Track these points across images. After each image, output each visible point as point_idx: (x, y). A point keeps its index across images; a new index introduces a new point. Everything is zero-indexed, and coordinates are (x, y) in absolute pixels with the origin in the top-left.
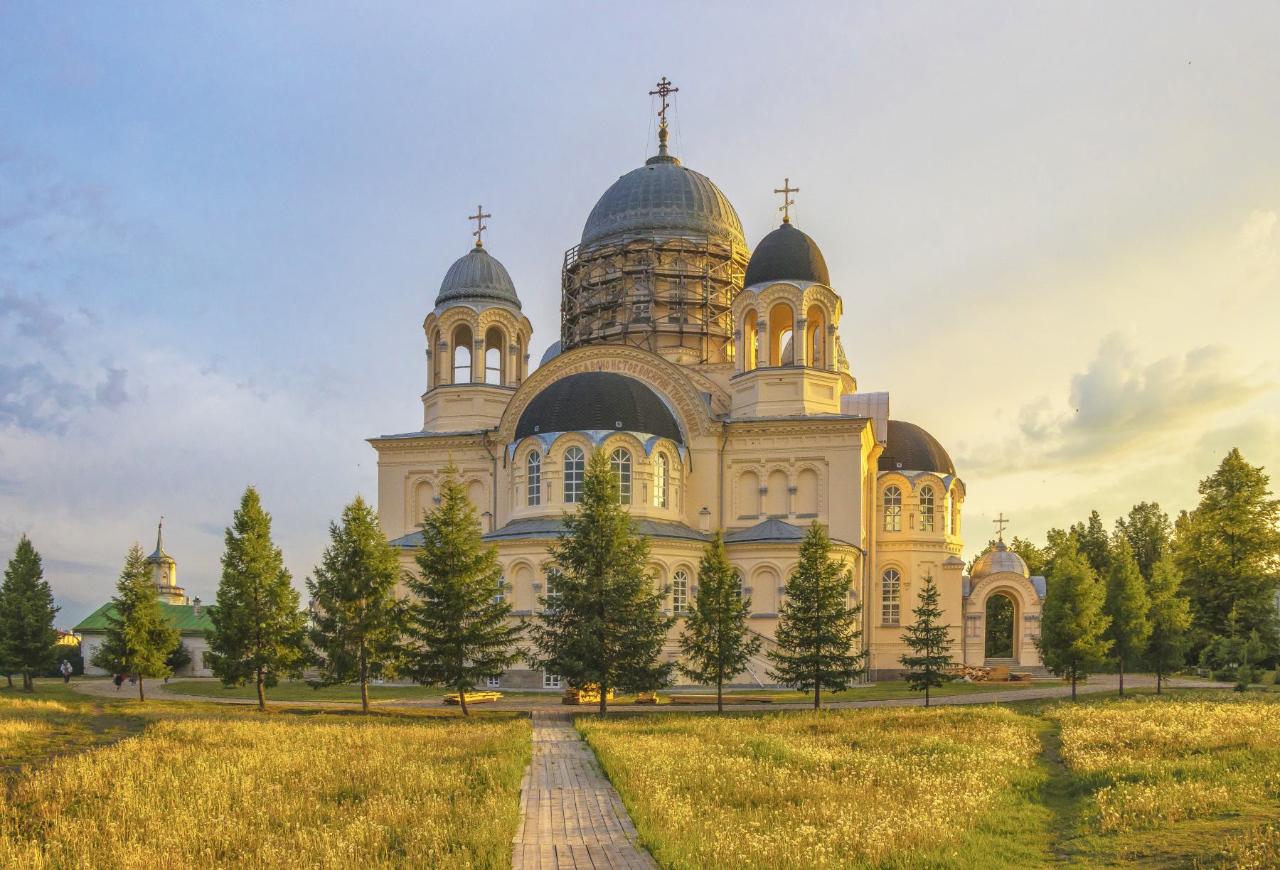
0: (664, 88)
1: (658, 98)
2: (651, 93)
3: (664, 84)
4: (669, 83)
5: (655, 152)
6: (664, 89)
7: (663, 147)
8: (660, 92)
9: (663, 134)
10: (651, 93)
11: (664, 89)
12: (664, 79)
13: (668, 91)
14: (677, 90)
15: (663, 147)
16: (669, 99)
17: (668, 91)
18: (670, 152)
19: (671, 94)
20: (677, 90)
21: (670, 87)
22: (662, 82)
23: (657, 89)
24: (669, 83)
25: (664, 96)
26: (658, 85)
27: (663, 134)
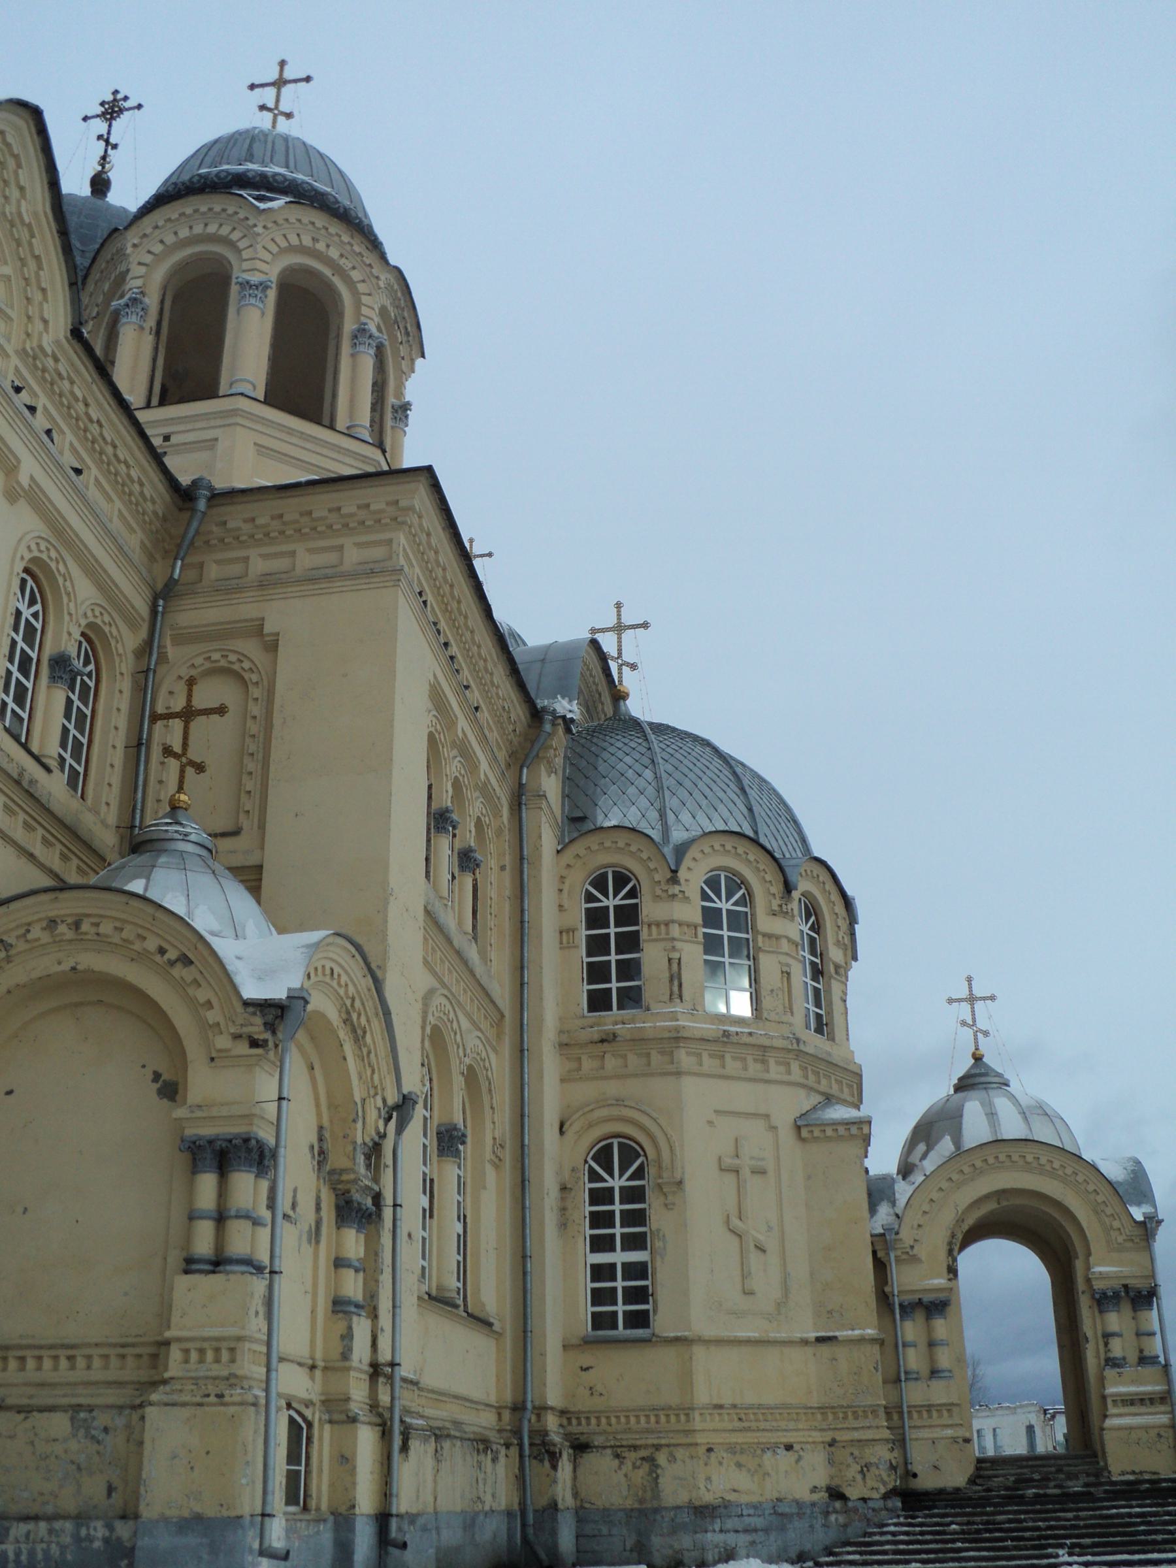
0: (114, 106)
1: (100, 126)
3: (115, 100)
4: (126, 98)
6: (112, 110)
8: (104, 114)
10: (85, 119)
11: (112, 110)
12: (116, 92)
14: (139, 107)
17: (121, 111)
19: (126, 115)
20: (139, 107)
21: (127, 104)
22: (110, 98)
23: (99, 110)
24: (126, 98)
25: (112, 118)
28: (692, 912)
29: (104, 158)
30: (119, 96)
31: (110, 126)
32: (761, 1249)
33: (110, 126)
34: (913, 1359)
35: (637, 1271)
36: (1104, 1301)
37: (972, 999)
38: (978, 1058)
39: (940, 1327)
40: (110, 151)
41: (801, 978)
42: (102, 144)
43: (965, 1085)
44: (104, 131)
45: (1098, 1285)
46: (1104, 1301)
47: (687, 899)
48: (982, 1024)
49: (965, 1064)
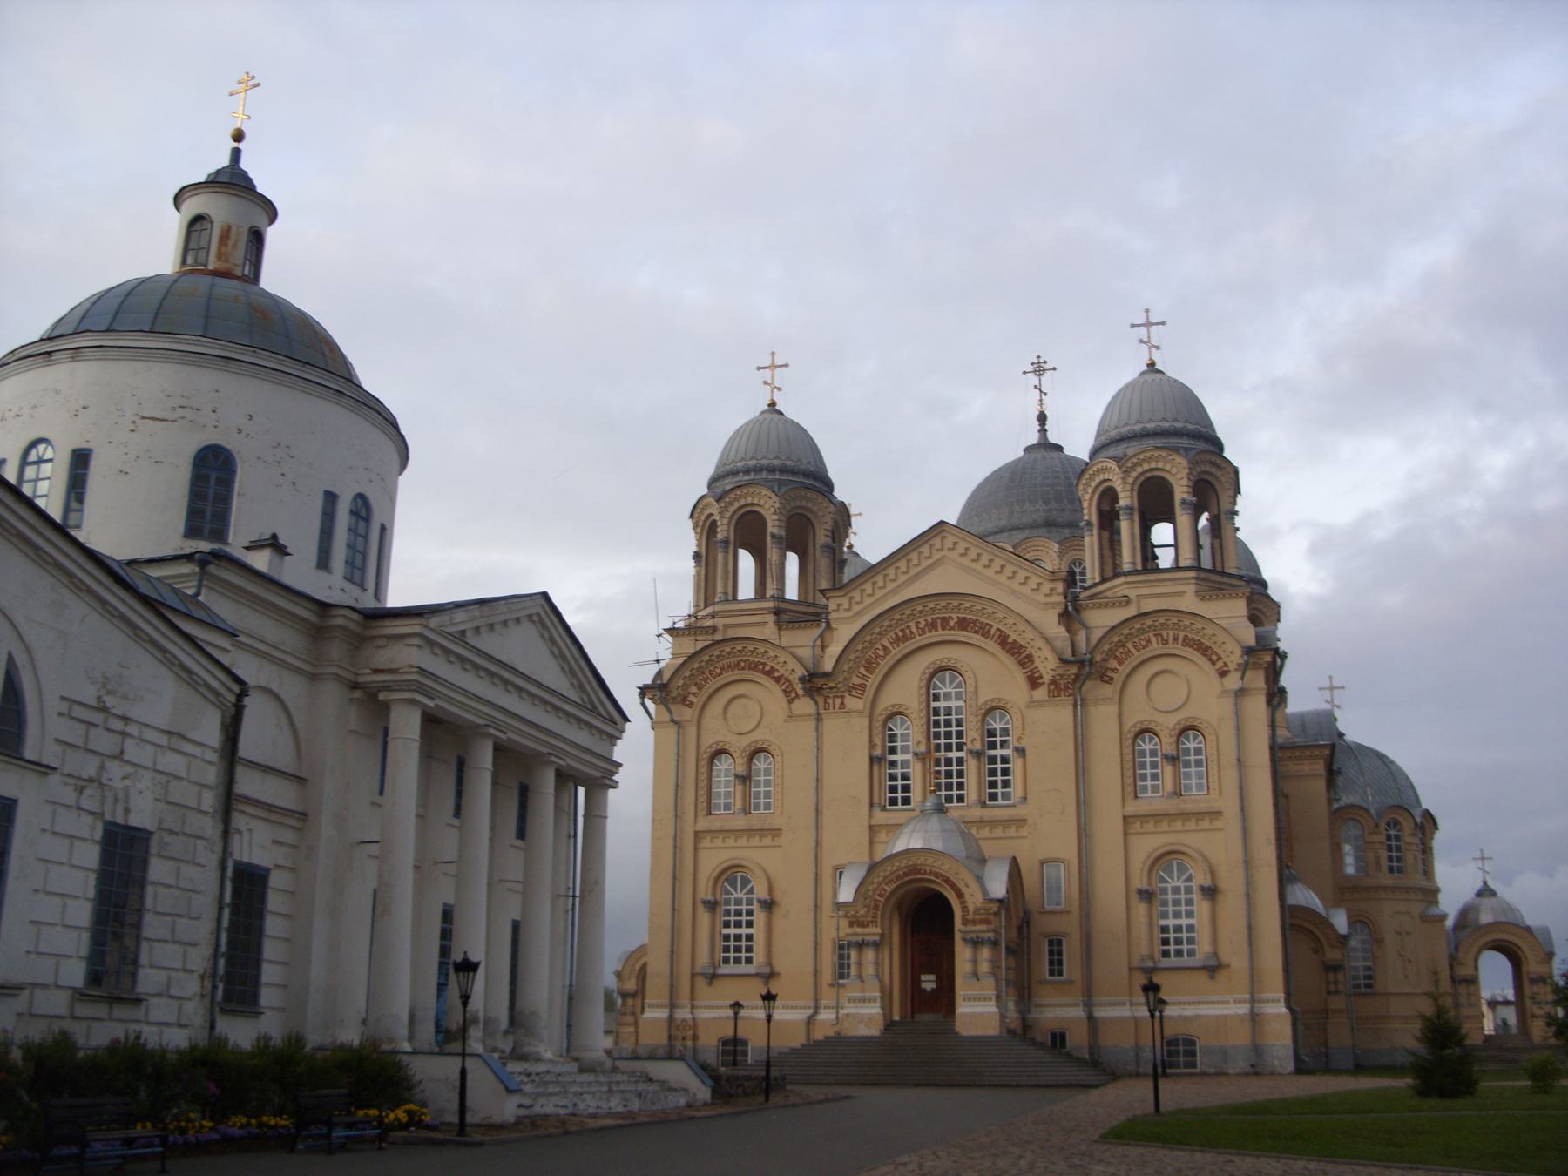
1: (1034, 379)
2: (1025, 373)
3: (1039, 363)
4: (1045, 362)
5: (1034, 439)
6: (1039, 369)
7: (1043, 431)
8: (1035, 371)
9: (1042, 418)
10: (1025, 373)
13: (1044, 370)
14: (1054, 369)
15: (1043, 431)
16: (1046, 377)
17: (1044, 370)
18: (1053, 438)
20: (1054, 369)
21: (1047, 366)
22: (1036, 361)
23: (1031, 368)
24: (1045, 362)
25: (1040, 375)
26: (1033, 364)
27: (1042, 418)
28: (1383, 839)
29: (1041, 400)
30: (1041, 360)
31: (1040, 380)
32: (1410, 961)
33: (1040, 380)
34: (1462, 1000)
35: (1369, 968)
36: (1533, 981)
37: (1483, 858)
38: (1485, 883)
39: (1472, 988)
40: (1043, 397)
41: (1420, 856)
42: (1037, 391)
43: (1479, 894)
44: (1037, 384)
45: (1531, 976)
46: (1533, 981)
47: (1380, 833)
48: (1487, 869)
49: (1478, 885)
